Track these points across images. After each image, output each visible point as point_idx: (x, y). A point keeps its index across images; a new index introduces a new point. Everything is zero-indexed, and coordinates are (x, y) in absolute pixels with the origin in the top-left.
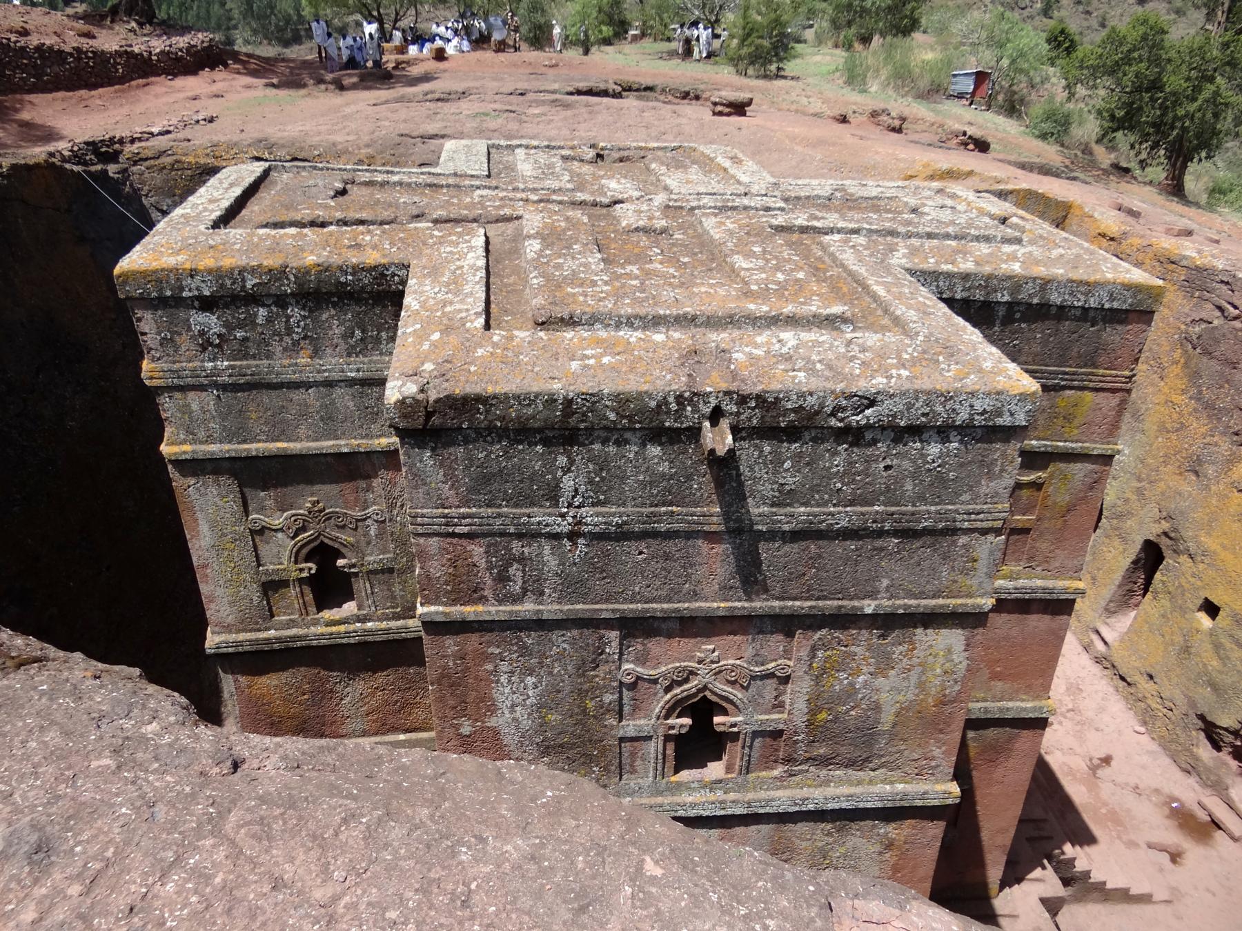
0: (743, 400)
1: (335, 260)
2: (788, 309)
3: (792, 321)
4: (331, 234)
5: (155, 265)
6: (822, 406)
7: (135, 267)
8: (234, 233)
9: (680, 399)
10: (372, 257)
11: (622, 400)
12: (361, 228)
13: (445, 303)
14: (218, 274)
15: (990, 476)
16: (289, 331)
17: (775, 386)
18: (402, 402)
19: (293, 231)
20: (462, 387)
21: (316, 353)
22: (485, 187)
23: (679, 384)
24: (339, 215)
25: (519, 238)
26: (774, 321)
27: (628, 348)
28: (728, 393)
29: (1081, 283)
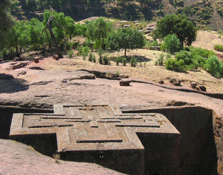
2: (113, 139)
7: (13, 134)
10: (50, 132)
19: (36, 128)
23: (96, 149)
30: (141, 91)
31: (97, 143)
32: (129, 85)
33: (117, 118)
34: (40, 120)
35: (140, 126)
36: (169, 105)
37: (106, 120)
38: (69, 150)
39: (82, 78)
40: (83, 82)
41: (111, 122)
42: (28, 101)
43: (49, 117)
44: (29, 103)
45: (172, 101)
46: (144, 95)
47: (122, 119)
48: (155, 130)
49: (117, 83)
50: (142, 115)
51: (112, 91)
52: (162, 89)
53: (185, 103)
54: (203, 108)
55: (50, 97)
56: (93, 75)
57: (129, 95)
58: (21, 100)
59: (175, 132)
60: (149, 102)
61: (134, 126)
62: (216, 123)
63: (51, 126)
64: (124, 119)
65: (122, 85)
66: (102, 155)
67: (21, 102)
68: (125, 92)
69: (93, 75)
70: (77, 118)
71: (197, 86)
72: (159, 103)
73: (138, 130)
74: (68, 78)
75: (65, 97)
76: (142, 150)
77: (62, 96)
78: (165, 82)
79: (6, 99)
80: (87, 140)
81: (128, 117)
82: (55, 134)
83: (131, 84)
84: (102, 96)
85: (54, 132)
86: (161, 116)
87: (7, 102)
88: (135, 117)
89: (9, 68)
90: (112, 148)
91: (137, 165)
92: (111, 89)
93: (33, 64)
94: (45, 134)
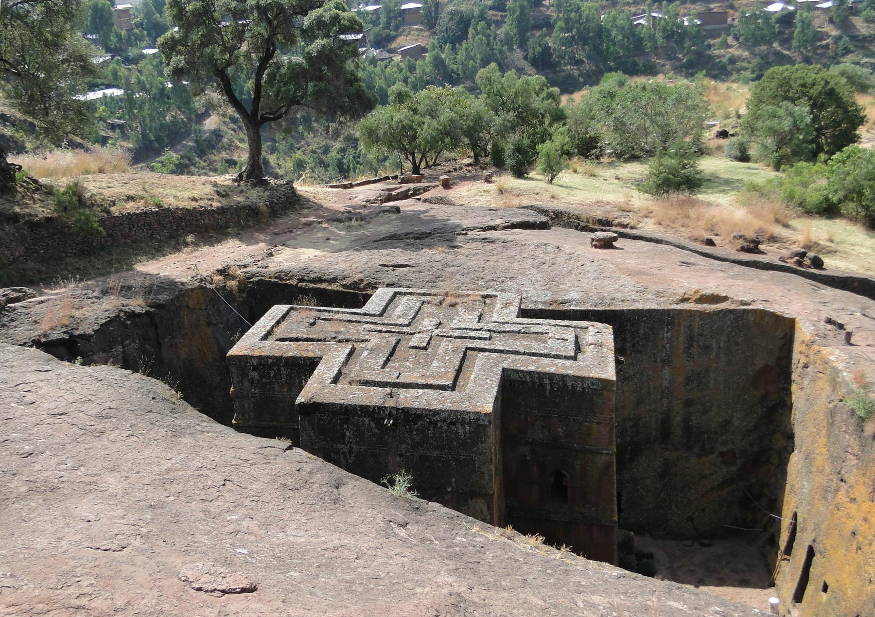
1: (299, 355)
4: (299, 345)
5: (240, 354)
6: (422, 413)
7: (233, 354)
8: (268, 343)
9: (379, 407)
14: (260, 358)
15: (482, 442)
17: (408, 406)
19: (287, 343)
22: (371, 323)
23: (379, 404)
24: (305, 336)
28: (393, 407)
29: (578, 377)
30: (632, 263)
31: (388, 390)
32: (612, 247)
34: (313, 324)
36: (684, 300)
37: (456, 333)
38: (318, 400)
39: (513, 226)
40: (504, 236)
41: (465, 338)
42: (361, 276)
43: (336, 316)
44: (362, 281)
45: (694, 290)
46: (632, 273)
47: (499, 332)
50: (556, 325)
51: (561, 259)
53: (725, 299)
54: (773, 315)
55: (413, 269)
58: (345, 273)
60: (637, 292)
61: (509, 352)
62: (801, 353)
63: (324, 340)
64: (504, 332)
65: (596, 247)
66: (390, 416)
67: (344, 278)
68: (588, 264)
69: (544, 219)
70: (391, 324)
72: (658, 294)
73: (510, 362)
74: (476, 225)
75: (447, 269)
76: (486, 415)
77: (440, 267)
79: (315, 270)
80: (373, 378)
81: (516, 328)
82: (321, 358)
83: (615, 244)
84: (534, 271)
85: (319, 354)
86: (604, 330)
87: (315, 275)
88: (534, 329)
89: (373, 198)
90: (416, 405)
91: (475, 449)
93: (438, 192)
94: (300, 358)
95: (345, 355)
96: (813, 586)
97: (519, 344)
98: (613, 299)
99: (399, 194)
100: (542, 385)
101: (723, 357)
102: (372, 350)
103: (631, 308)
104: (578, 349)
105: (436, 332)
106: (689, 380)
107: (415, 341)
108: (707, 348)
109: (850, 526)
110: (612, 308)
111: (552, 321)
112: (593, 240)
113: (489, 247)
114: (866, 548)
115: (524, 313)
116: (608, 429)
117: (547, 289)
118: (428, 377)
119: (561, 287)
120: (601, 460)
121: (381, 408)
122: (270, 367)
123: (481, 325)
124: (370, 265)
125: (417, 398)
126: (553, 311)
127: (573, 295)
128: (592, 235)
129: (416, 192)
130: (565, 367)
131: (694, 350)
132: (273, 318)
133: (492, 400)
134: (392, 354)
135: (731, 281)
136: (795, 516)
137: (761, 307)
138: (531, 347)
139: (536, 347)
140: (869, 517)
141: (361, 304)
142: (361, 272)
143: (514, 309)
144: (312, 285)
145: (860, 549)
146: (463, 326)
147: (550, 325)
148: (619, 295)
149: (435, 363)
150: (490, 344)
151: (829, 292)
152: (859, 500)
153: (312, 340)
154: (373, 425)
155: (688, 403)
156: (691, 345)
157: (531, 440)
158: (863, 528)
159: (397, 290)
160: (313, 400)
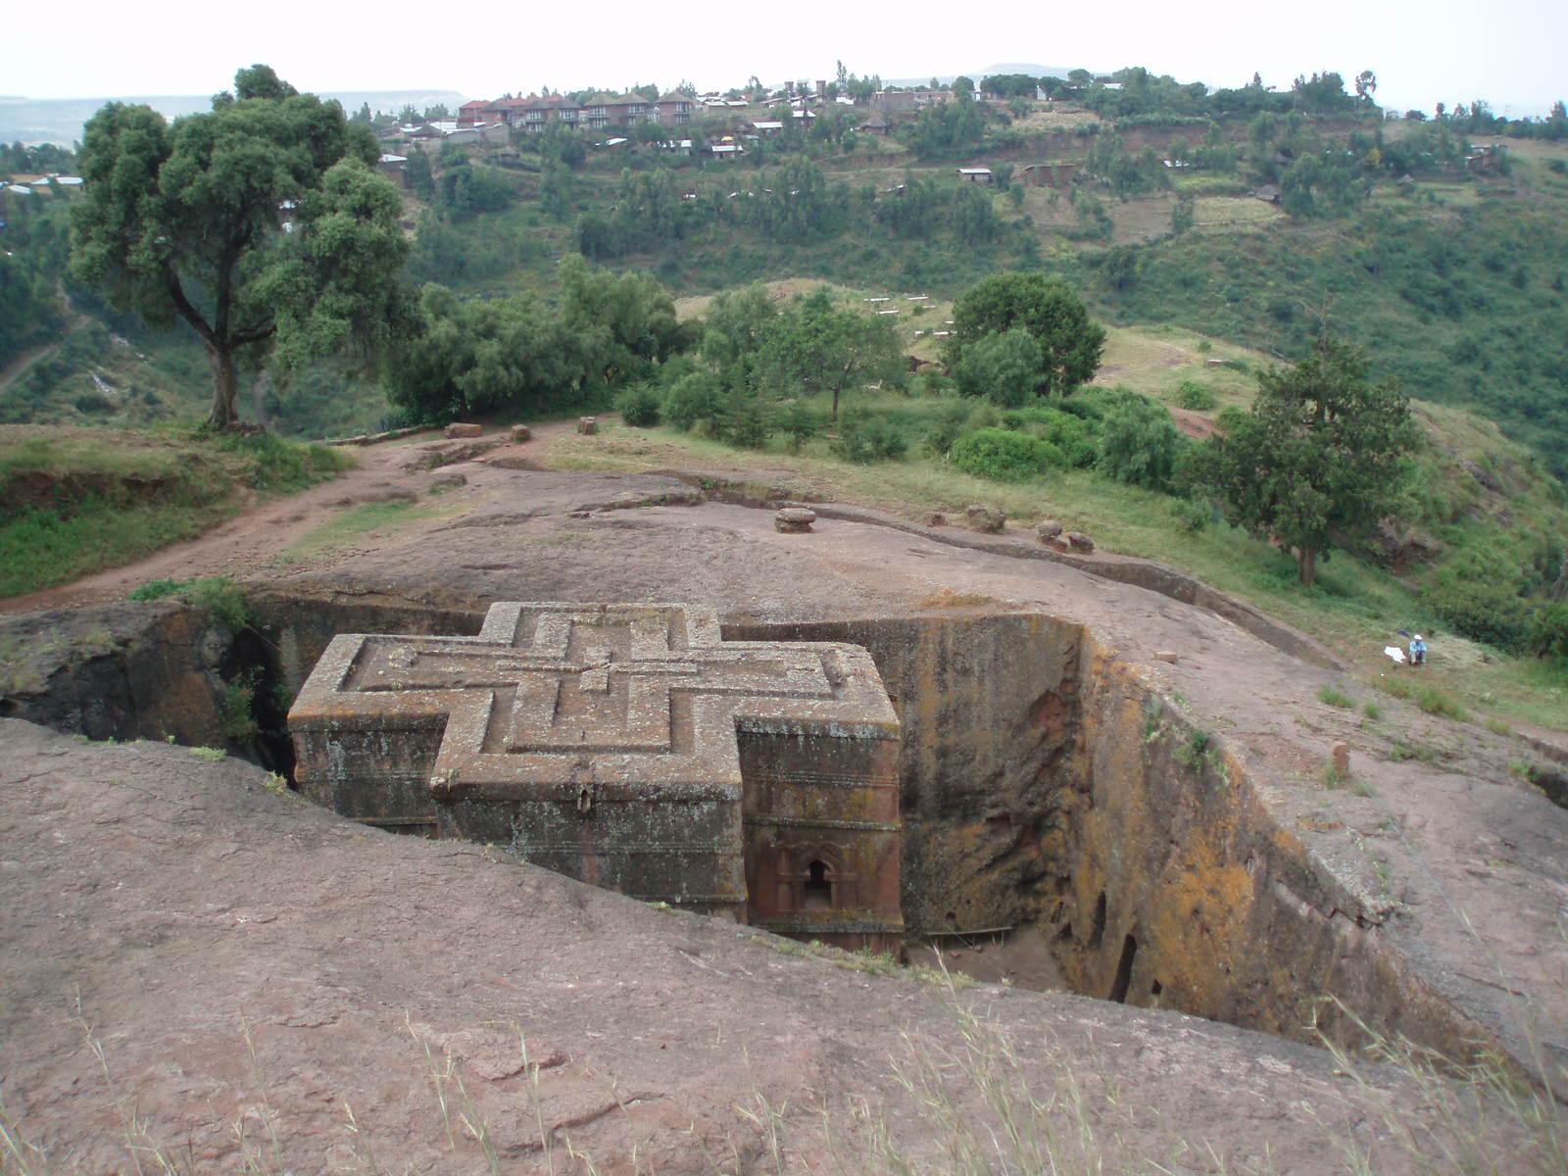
0: (596, 787)
3: (638, 749)
5: (310, 713)
8: (352, 695)
10: (428, 710)
11: (540, 786)
12: (424, 691)
13: (466, 738)
14: (343, 719)
15: (729, 827)
16: (380, 749)
17: (612, 780)
18: (436, 787)
19: (384, 693)
20: (464, 779)
21: (395, 764)
22: (506, 657)
24: (411, 682)
25: (514, 697)
26: (627, 749)
27: (546, 762)
30: (844, 553)
31: (575, 757)
32: (809, 530)
33: (692, 661)
35: (759, 693)
40: (646, 518)
46: (850, 568)
48: (810, 708)
49: (770, 516)
51: (740, 552)
52: (926, 545)
53: (988, 600)
56: (694, 491)
57: (794, 566)
59: (883, 720)
62: (1097, 673)
63: (441, 687)
65: (783, 530)
68: (783, 557)
69: (694, 491)
71: (1063, 538)
72: (893, 597)
76: (735, 785)
77: (558, 567)
78: (949, 516)
81: (732, 657)
82: (447, 716)
92: (739, 543)
95: (488, 709)
96: (1137, 990)
97: (747, 680)
98: (828, 607)
99: (450, 454)
100: (793, 736)
101: (988, 684)
102: (526, 699)
103: (856, 619)
104: (837, 682)
105: (614, 666)
106: (942, 720)
107: (587, 682)
108: (966, 672)
109: (1186, 903)
110: (830, 620)
111: (777, 643)
112: (778, 519)
113: (627, 535)
114: (1217, 929)
115: (727, 634)
116: (889, 796)
117: (727, 597)
118: (629, 735)
119: (748, 591)
120: (879, 842)
121: (570, 786)
122: (362, 733)
123: (676, 654)
124: (447, 565)
125: (624, 767)
126: (759, 629)
127: (768, 604)
128: (777, 514)
129: (477, 451)
130: (824, 711)
131: (949, 676)
132: (345, 656)
133: (736, 764)
134: (558, 705)
135: (987, 576)
136: (1102, 901)
137: (1037, 611)
138: (765, 684)
139: (774, 684)
140: (1218, 887)
141: (477, 632)
142: (434, 579)
143: (714, 625)
144: (356, 602)
145: (1208, 931)
146: (650, 656)
147: (778, 649)
148: (835, 601)
149: (632, 714)
150: (704, 682)
151: (1112, 587)
152: (1200, 865)
153: (423, 687)
154: (556, 812)
155: (943, 753)
156: (944, 670)
157: (775, 820)
158: (1209, 903)
159: (523, 604)
160: (458, 780)
